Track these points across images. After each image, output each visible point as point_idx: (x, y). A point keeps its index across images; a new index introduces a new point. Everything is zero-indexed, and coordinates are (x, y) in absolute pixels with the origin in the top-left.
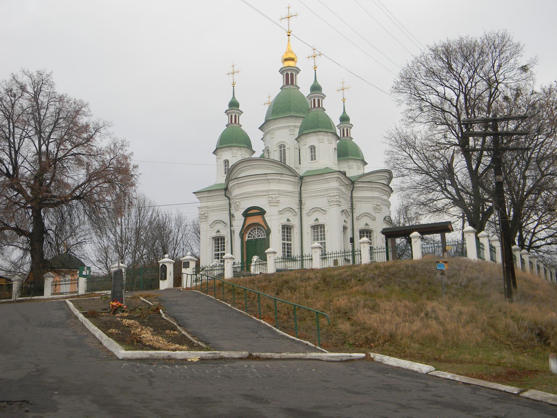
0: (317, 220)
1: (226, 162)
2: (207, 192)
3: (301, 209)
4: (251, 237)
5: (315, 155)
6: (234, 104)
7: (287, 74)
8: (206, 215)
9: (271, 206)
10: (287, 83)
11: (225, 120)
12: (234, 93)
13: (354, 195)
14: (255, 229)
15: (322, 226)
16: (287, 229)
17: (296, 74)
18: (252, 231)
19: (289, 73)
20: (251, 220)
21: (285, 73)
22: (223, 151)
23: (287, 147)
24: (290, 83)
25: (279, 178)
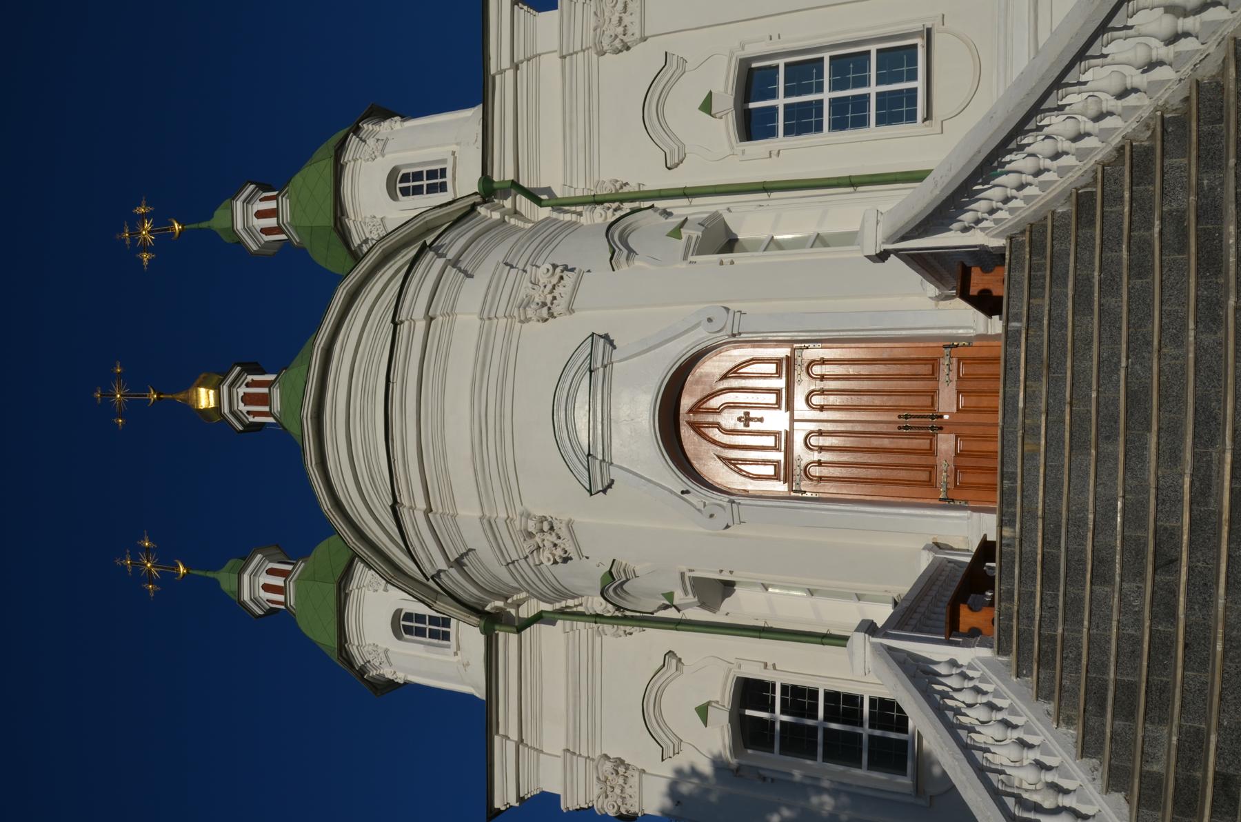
0: (707, 106)
5: (432, 174)
8: (608, 766)
9: (570, 310)
21: (242, 407)
22: (360, 636)
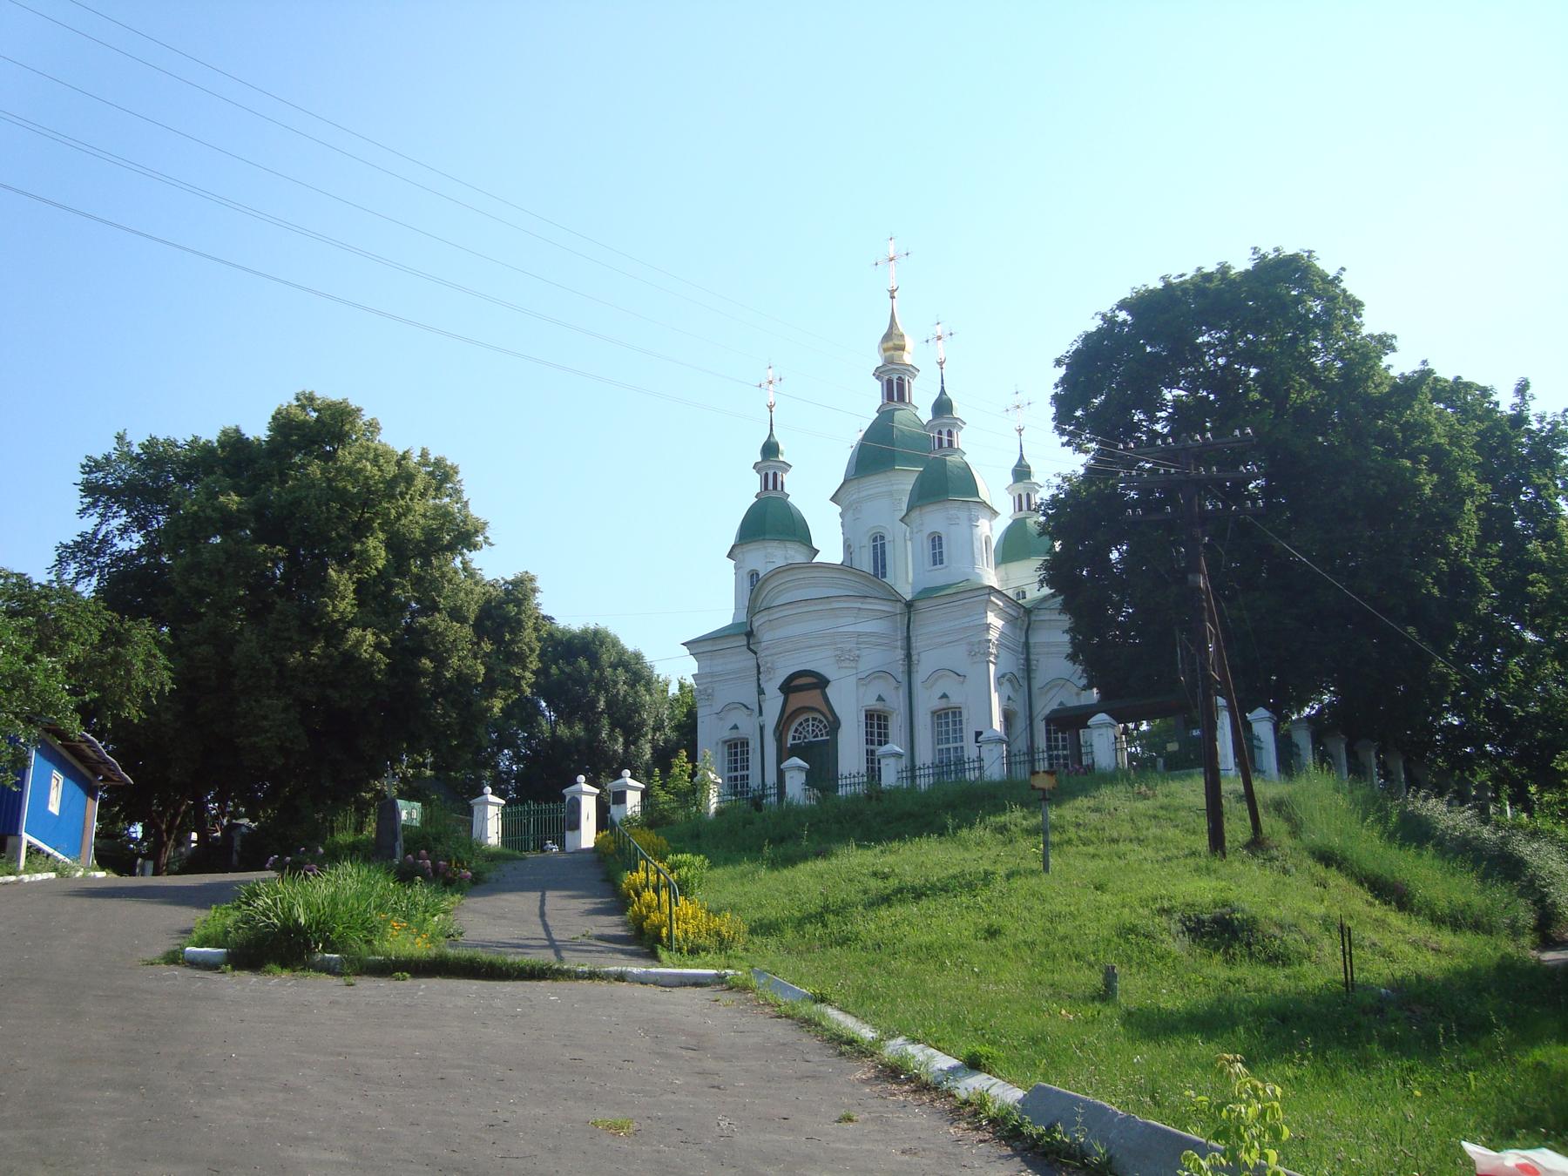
0: (944, 696)
1: (754, 575)
2: (710, 642)
3: (909, 673)
4: (799, 739)
5: (941, 553)
6: (770, 449)
7: (890, 382)
10: (890, 397)
11: (754, 484)
12: (771, 425)
13: (1032, 641)
14: (807, 720)
15: (957, 712)
16: (879, 718)
17: (911, 380)
18: (801, 724)
19: (895, 377)
20: (798, 700)
23: (888, 538)
24: (896, 399)
25: (859, 605)
